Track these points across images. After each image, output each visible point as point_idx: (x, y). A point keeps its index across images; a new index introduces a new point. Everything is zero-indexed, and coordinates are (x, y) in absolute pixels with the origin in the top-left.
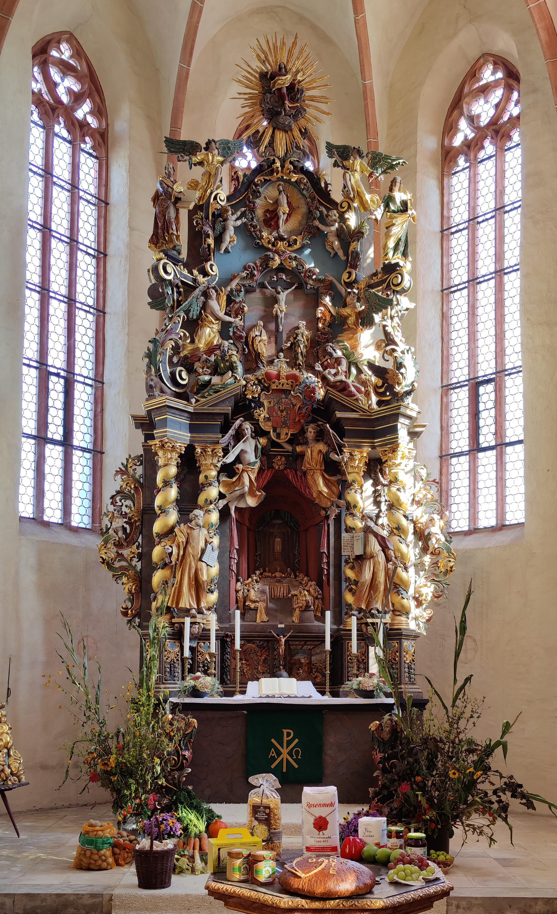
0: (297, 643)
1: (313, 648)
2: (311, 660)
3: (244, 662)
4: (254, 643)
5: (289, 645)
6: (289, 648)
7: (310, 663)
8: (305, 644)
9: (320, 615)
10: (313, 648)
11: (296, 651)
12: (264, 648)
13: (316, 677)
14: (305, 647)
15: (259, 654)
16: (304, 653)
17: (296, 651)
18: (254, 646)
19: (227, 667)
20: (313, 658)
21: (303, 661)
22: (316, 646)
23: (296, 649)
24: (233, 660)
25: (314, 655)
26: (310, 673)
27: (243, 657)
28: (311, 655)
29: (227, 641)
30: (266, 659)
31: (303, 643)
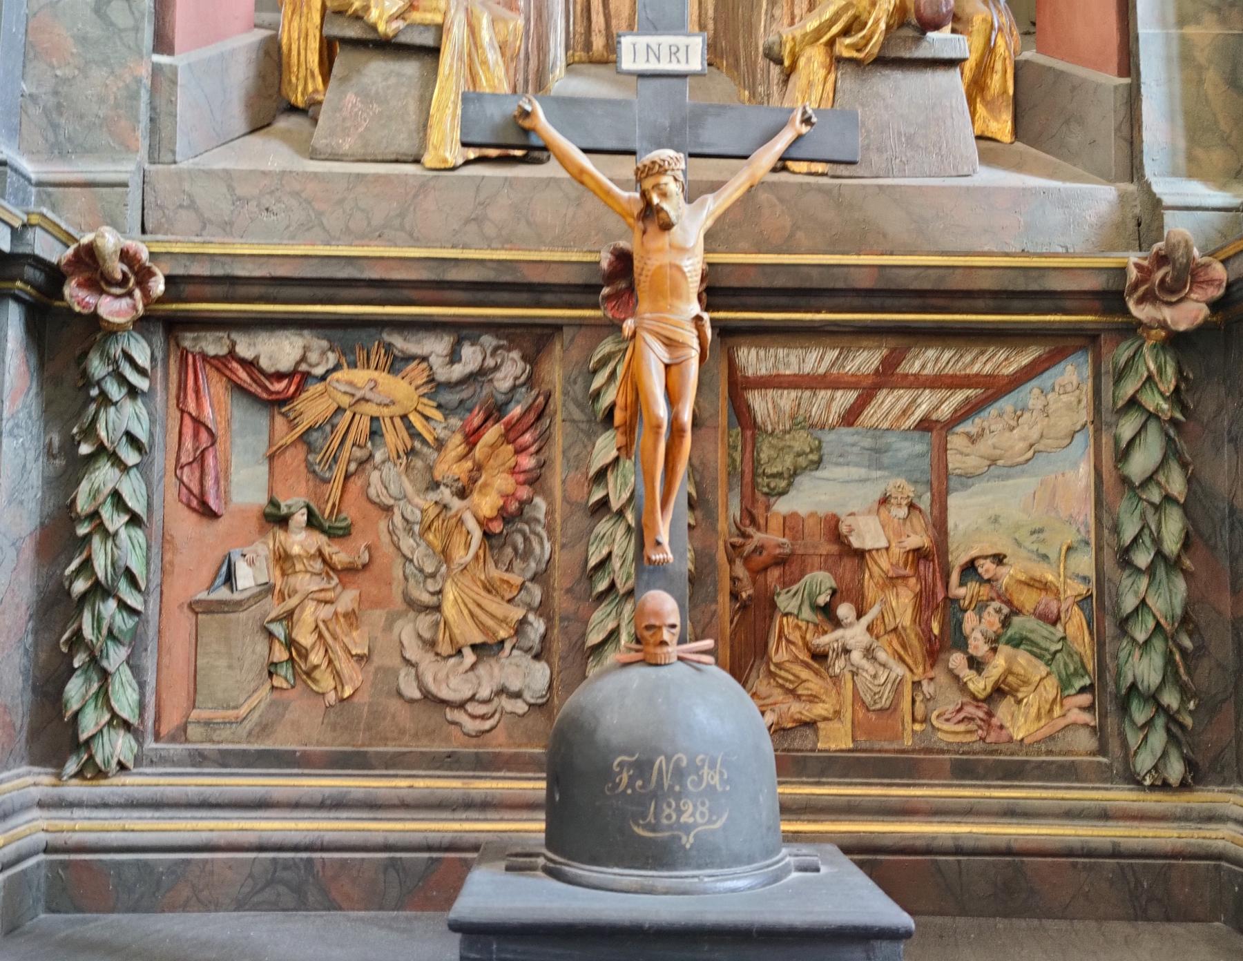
0: (812, 360)
1: (961, 415)
2: (940, 526)
3: (299, 540)
4: (397, 363)
5: (738, 387)
6: (742, 414)
7: (929, 558)
8: (887, 377)
9: (1002, 127)
10: (961, 415)
11: (801, 441)
12: (495, 411)
13: (999, 692)
14: (887, 403)
15: (451, 466)
16: (876, 456)
17: (801, 441)
18: (401, 390)
19: (100, 590)
20: (964, 511)
21: (868, 533)
22: (995, 389)
23: (800, 422)
24: (185, 524)
25: (968, 478)
26: (934, 652)
27: (294, 501)
28: (941, 484)
29: (112, 332)
30: (512, 515)
31: (865, 360)
